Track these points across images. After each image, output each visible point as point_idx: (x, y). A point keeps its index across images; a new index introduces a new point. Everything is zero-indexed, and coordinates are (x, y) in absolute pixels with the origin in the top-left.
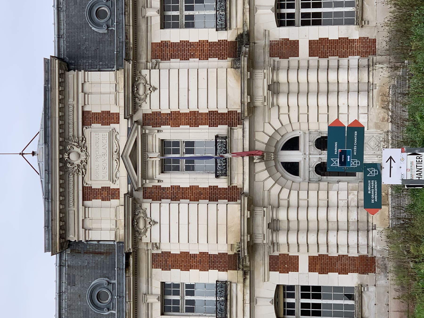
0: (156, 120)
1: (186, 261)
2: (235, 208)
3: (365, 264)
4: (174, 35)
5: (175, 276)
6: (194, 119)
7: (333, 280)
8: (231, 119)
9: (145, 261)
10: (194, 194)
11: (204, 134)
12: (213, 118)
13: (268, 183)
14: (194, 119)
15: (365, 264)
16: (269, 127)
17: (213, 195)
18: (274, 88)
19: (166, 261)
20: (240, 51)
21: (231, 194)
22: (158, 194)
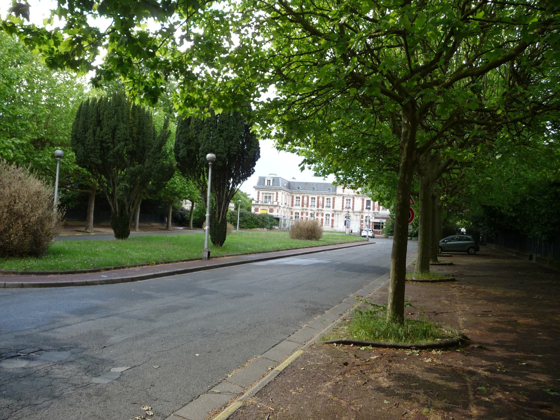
0: (354, 198)
1: (334, 202)
2: (341, 209)
3: (332, 226)
4: (365, 202)
5: (332, 201)
6: (353, 204)
7: (330, 222)
8: (353, 209)
9: (334, 196)
10: (343, 204)
11: (351, 206)
12: (353, 207)
13: (344, 214)
14: (353, 204)
15: (332, 226)
16: (351, 214)
17: (343, 206)
18: (357, 215)
19: (334, 199)
20: (362, 211)
21: (343, 209)
22: (343, 198)
